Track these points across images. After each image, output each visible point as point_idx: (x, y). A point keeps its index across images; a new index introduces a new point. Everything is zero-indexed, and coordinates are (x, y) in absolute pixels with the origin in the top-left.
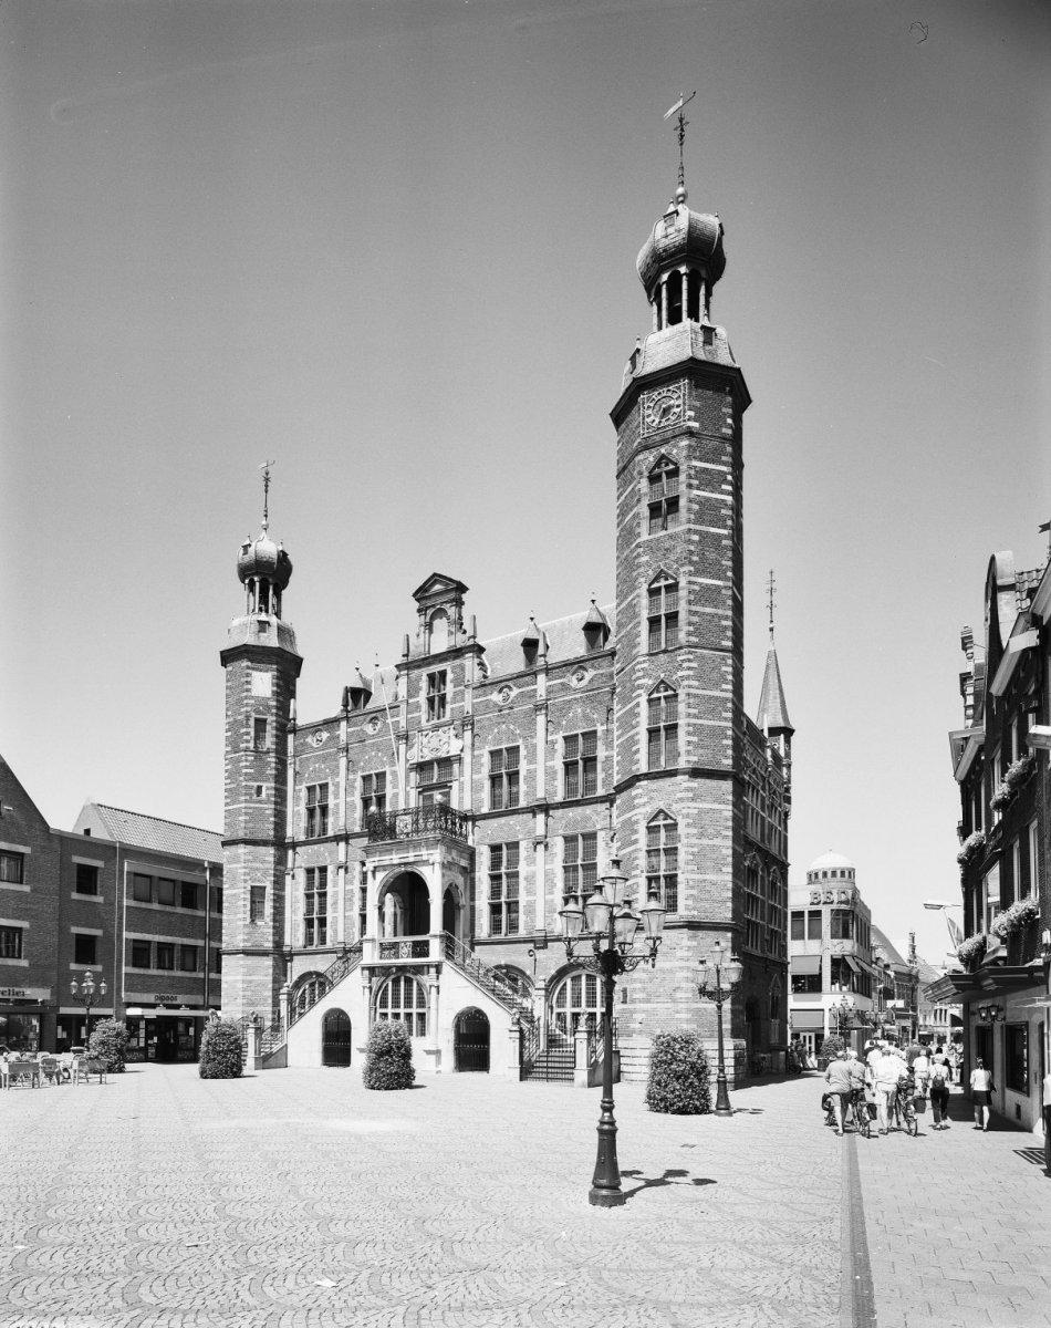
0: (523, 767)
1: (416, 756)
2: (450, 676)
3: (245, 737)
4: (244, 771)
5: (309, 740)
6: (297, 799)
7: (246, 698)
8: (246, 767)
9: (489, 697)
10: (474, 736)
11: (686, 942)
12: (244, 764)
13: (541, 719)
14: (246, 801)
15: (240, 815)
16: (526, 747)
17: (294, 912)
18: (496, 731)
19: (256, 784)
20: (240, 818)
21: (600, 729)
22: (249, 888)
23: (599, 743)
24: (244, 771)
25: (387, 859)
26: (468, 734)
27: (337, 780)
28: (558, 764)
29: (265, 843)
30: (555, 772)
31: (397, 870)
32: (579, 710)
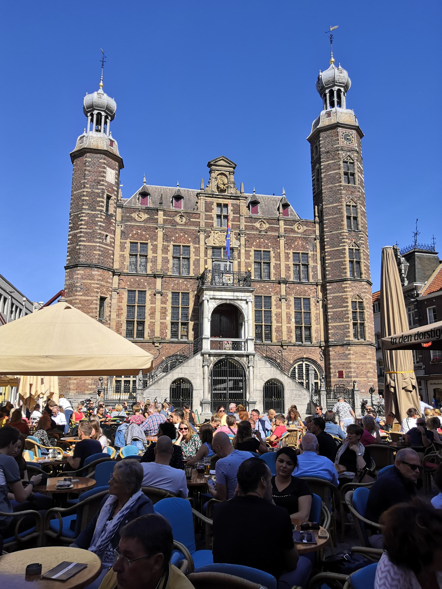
0: (273, 262)
1: (211, 242)
2: (230, 208)
3: (101, 204)
4: (99, 224)
5: (133, 215)
6: (122, 248)
7: (103, 181)
8: (101, 222)
9: (254, 224)
10: (246, 240)
11: (370, 352)
13: (282, 241)
14: (100, 242)
15: (95, 250)
16: (274, 253)
17: (118, 315)
18: (258, 241)
19: (105, 233)
20: (95, 252)
21: (310, 253)
22: (99, 297)
23: (310, 259)
24: (99, 224)
25: (218, 294)
26: (243, 239)
27: (155, 243)
28: (291, 263)
29: (109, 270)
30: (289, 267)
31: (224, 302)
32: (300, 242)
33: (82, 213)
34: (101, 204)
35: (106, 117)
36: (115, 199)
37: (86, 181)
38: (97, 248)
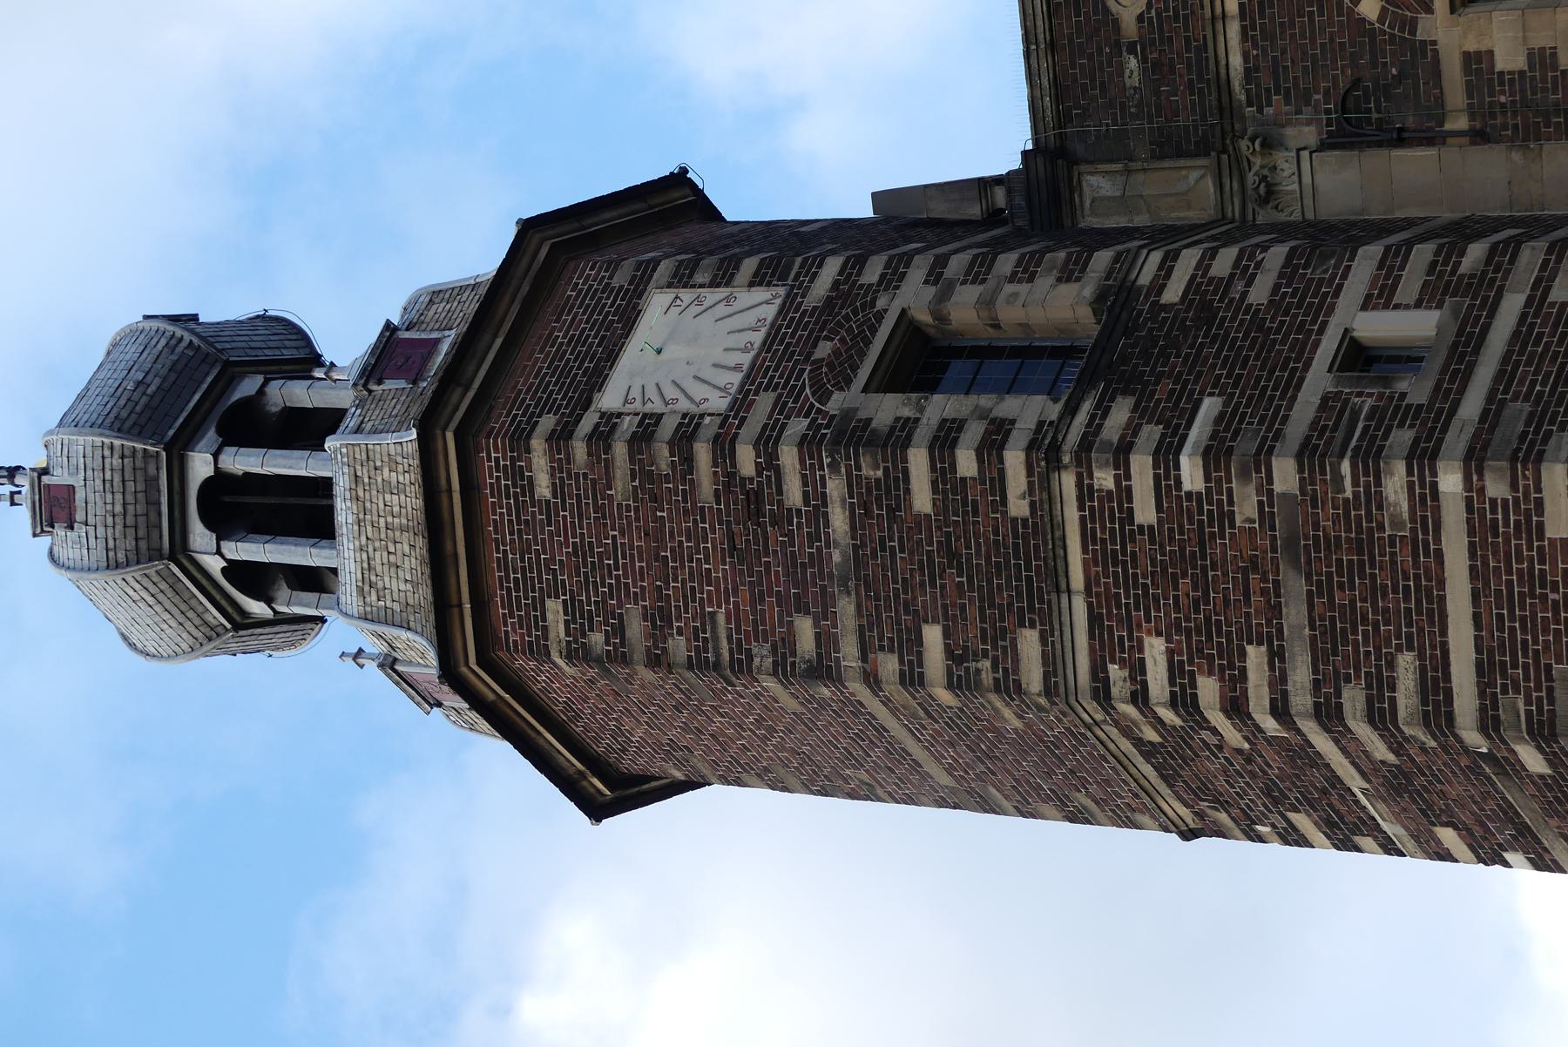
3: (966, 463)
4: (1191, 474)
7: (724, 447)
12: (1142, 467)
14: (1424, 457)
24: (1191, 474)
33: (1102, 692)
34: (966, 463)
35: (249, 426)
36: (934, 276)
37: (762, 655)
38: (1496, 488)
